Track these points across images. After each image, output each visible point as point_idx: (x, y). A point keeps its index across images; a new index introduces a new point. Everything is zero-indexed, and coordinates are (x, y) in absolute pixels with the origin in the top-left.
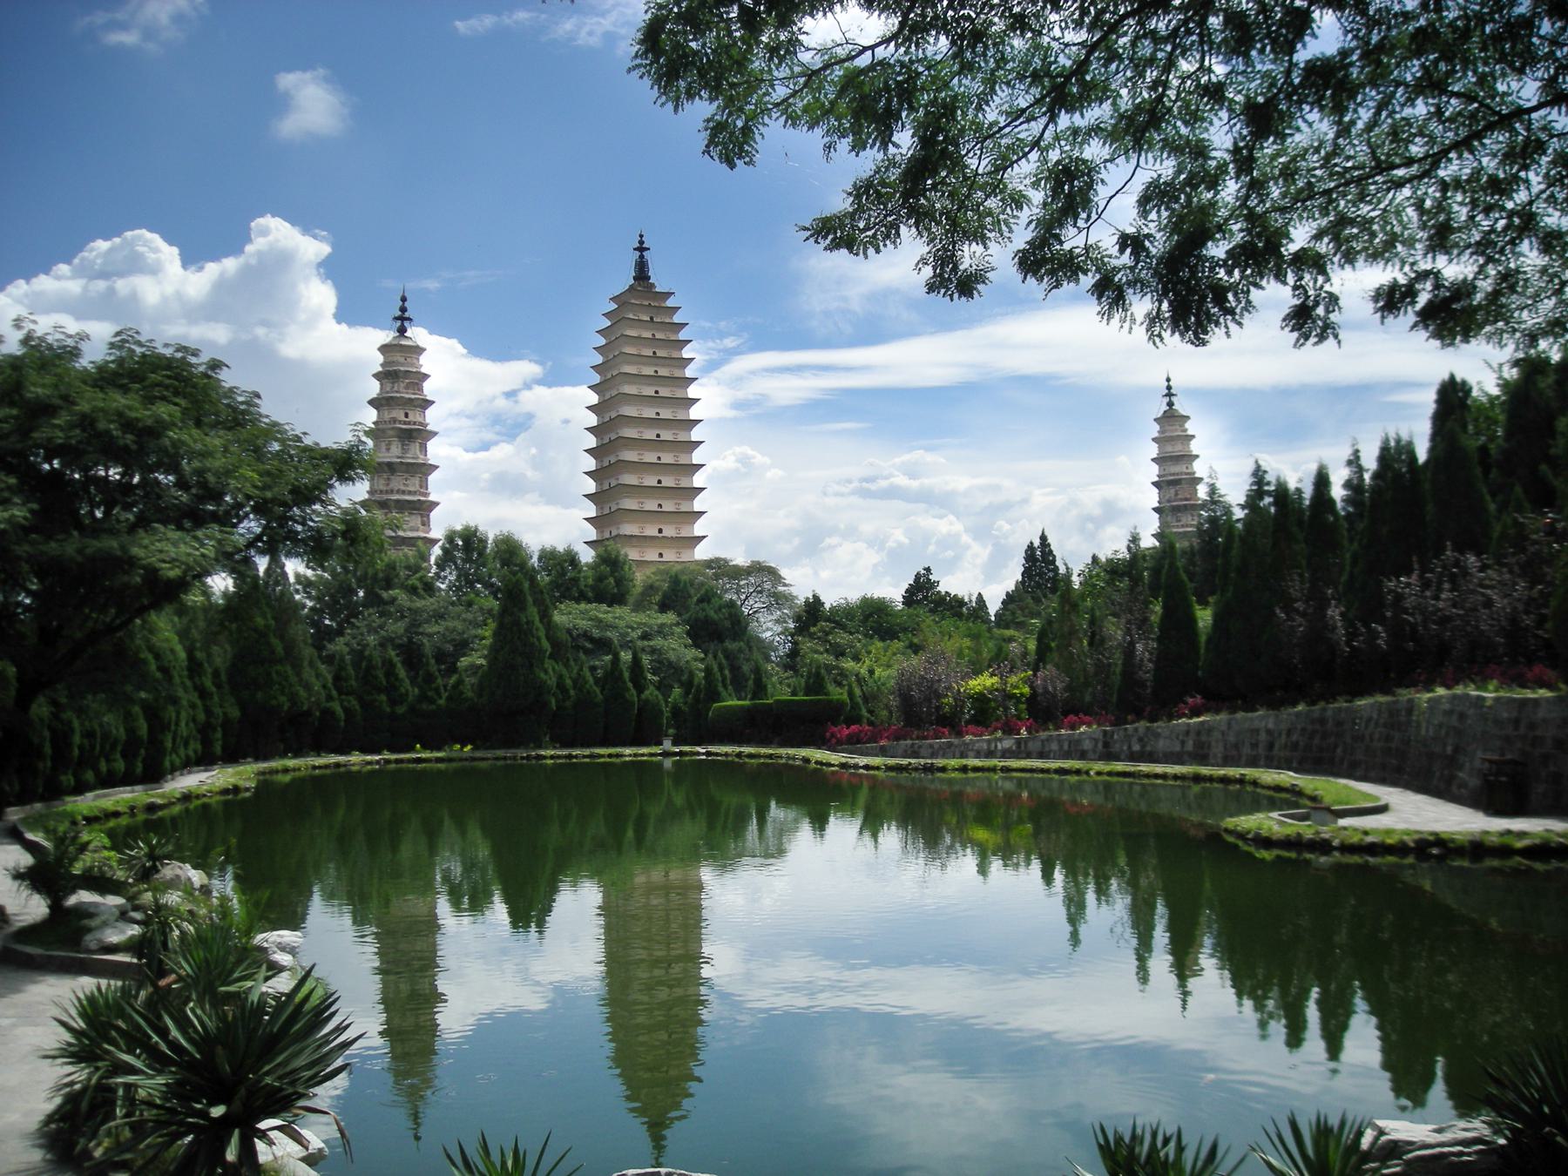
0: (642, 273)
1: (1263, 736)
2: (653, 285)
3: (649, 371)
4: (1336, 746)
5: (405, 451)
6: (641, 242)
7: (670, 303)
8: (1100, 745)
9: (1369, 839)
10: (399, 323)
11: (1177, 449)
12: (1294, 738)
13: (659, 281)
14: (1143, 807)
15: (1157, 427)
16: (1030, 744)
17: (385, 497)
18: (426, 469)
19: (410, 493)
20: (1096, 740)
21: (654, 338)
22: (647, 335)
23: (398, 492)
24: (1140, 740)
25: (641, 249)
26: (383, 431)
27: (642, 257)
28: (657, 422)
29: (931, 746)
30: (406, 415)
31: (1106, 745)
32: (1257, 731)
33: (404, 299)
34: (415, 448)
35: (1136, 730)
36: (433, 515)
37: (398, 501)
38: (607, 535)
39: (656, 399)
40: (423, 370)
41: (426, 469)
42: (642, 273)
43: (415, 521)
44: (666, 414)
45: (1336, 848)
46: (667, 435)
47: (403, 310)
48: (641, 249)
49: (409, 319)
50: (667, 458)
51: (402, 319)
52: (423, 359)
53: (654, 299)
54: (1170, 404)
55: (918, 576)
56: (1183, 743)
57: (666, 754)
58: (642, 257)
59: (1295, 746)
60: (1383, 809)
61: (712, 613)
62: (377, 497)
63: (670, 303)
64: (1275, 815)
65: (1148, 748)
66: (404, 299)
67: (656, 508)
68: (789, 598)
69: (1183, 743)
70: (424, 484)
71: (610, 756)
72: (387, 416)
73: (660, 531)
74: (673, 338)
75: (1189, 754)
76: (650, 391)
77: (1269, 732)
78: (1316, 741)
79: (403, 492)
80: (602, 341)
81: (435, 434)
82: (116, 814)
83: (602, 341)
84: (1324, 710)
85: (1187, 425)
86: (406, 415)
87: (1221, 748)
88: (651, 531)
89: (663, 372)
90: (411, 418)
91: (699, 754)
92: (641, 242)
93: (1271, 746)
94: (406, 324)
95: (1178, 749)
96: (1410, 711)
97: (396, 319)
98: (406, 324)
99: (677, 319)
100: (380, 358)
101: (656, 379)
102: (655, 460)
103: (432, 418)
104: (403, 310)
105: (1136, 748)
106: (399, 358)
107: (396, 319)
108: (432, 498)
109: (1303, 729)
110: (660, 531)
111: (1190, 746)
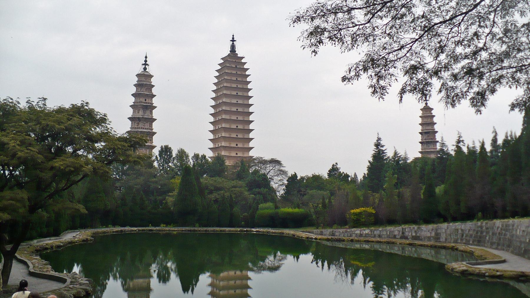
1: (460, 231)
2: (237, 54)
3: (234, 85)
4: (486, 236)
5: (144, 113)
6: (233, 38)
7: (243, 61)
8: (401, 233)
9: (498, 273)
10: (144, 66)
11: (429, 121)
12: (471, 232)
13: (240, 52)
14: (416, 256)
15: (421, 112)
16: (375, 232)
17: (136, 130)
19: (146, 129)
20: (399, 231)
23: (141, 128)
24: (415, 232)
25: (233, 40)
27: (233, 43)
28: (237, 105)
30: (145, 100)
31: (403, 233)
32: (458, 230)
33: (146, 57)
34: (148, 112)
35: (414, 228)
36: (154, 137)
37: (141, 132)
38: (217, 146)
39: (237, 96)
40: (152, 84)
45: (487, 276)
46: (240, 110)
47: (146, 61)
48: (233, 40)
49: (148, 65)
52: (152, 80)
53: (237, 59)
55: (333, 165)
56: (431, 233)
58: (233, 43)
59: (471, 235)
60: (504, 261)
61: (257, 178)
62: (133, 130)
63: (243, 61)
64: (464, 263)
65: (418, 235)
66: (146, 57)
67: (235, 136)
68: (284, 173)
69: (431, 233)
70: (151, 125)
71: (221, 231)
72: (138, 101)
73: (237, 145)
75: (433, 237)
76: (234, 93)
77: (462, 230)
78: (479, 234)
79: (143, 128)
80: (217, 74)
81: (156, 107)
82: (47, 249)
83: (217, 74)
84: (482, 223)
85: (432, 112)
86: (145, 100)
87: (444, 235)
88: (233, 145)
91: (253, 231)
92: (233, 38)
93: (463, 236)
94: (147, 66)
95: (429, 235)
96: (513, 225)
98: (147, 66)
99: (246, 67)
100: (137, 79)
103: (155, 101)
104: (146, 61)
105: (414, 234)
106: (143, 79)
107: (143, 64)
108: (153, 131)
109: (474, 230)
110: (237, 145)
111: (433, 234)
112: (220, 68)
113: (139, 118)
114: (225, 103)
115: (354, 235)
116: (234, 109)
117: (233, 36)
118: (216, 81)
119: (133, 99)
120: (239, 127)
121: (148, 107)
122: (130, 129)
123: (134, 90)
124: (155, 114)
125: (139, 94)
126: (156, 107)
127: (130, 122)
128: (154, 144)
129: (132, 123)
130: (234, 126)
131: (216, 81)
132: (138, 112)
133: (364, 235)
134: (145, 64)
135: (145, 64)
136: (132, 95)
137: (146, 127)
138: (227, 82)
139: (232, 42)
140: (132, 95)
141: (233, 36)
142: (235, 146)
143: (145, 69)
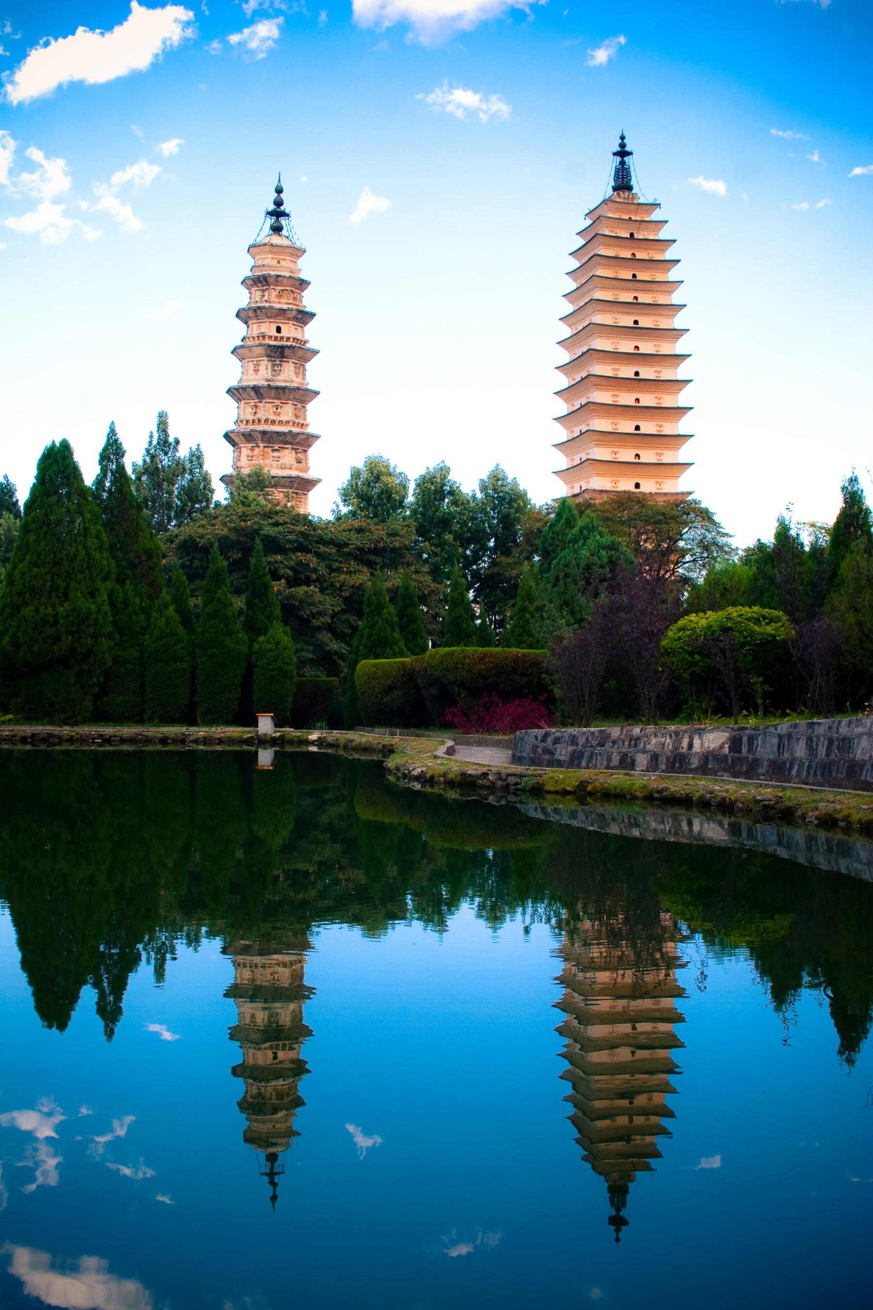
0: (623, 182)
2: (634, 196)
3: (627, 297)
6: (622, 146)
7: (656, 216)
17: (251, 427)
18: (302, 396)
21: (634, 259)
22: (627, 254)
25: (623, 153)
26: (250, 348)
27: (623, 163)
29: (573, 740)
30: (279, 330)
33: (279, 191)
36: (311, 451)
37: (264, 433)
41: (302, 396)
42: (623, 182)
43: (288, 456)
44: (647, 347)
46: (647, 373)
47: (279, 203)
48: (623, 153)
50: (648, 400)
57: (263, 741)
58: (623, 163)
62: (243, 428)
63: (656, 216)
66: (279, 191)
67: (632, 459)
72: (255, 333)
74: (657, 257)
76: (628, 321)
81: (315, 352)
83: (576, 264)
86: (279, 330)
89: (644, 298)
90: (285, 333)
92: (622, 146)
98: (283, 221)
99: (663, 235)
101: (635, 304)
102: (632, 403)
104: (279, 203)
106: (269, 260)
107: (271, 214)
108: (310, 430)
112: (584, 242)
113: (256, 389)
114: (591, 354)
115: (642, 760)
116: (627, 371)
117: (622, 138)
119: (241, 330)
120: (643, 431)
121: (287, 352)
122: (233, 427)
123: (243, 298)
124: (315, 375)
126: (315, 352)
127: (232, 403)
128: (311, 474)
130: (627, 426)
132: (256, 371)
133: (695, 763)
134: (278, 213)
135: (278, 213)
138: (603, 288)
139: (619, 159)
141: (622, 138)
142: (633, 489)
143: (277, 229)
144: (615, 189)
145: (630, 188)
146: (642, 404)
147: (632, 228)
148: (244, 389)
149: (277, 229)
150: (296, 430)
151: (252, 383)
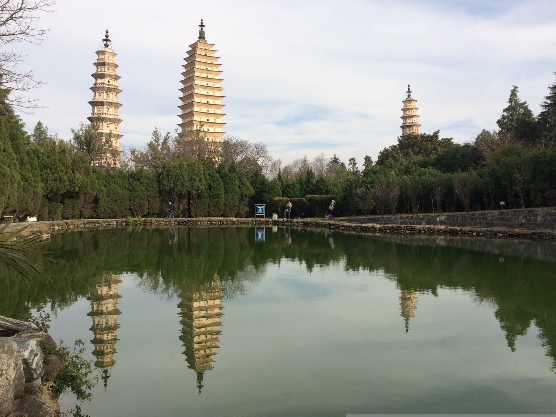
0: (202, 36)
2: (206, 41)
3: (204, 75)
6: (202, 23)
7: (213, 48)
10: (105, 42)
15: (404, 105)
22: (204, 61)
25: (202, 26)
26: (99, 88)
27: (202, 29)
28: (208, 96)
30: (109, 82)
33: (107, 32)
39: (207, 87)
42: (202, 36)
44: (211, 93)
47: (107, 36)
48: (202, 26)
49: (109, 41)
51: (107, 40)
54: (409, 96)
58: (202, 29)
62: (96, 116)
66: (107, 32)
76: (204, 84)
86: (109, 82)
89: (210, 76)
90: (111, 83)
92: (202, 23)
97: (104, 40)
98: (108, 43)
99: (216, 55)
104: (107, 36)
107: (104, 40)
117: (202, 20)
118: (184, 70)
125: (100, 74)
129: (94, 108)
131: (184, 70)
134: (107, 40)
136: (93, 75)
137: (111, 113)
139: (200, 28)
140: (93, 75)
141: (202, 20)
143: (106, 46)
144: (199, 38)
145: (204, 38)
146: (209, 112)
147: (206, 52)
148: (97, 102)
149: (106, 46)
150: (116, 117)
151: (100, 100)
